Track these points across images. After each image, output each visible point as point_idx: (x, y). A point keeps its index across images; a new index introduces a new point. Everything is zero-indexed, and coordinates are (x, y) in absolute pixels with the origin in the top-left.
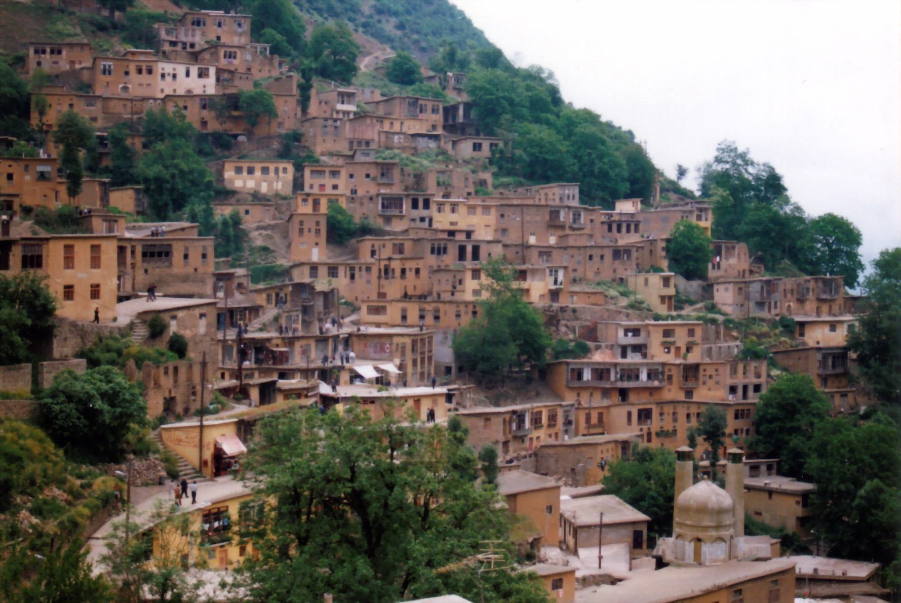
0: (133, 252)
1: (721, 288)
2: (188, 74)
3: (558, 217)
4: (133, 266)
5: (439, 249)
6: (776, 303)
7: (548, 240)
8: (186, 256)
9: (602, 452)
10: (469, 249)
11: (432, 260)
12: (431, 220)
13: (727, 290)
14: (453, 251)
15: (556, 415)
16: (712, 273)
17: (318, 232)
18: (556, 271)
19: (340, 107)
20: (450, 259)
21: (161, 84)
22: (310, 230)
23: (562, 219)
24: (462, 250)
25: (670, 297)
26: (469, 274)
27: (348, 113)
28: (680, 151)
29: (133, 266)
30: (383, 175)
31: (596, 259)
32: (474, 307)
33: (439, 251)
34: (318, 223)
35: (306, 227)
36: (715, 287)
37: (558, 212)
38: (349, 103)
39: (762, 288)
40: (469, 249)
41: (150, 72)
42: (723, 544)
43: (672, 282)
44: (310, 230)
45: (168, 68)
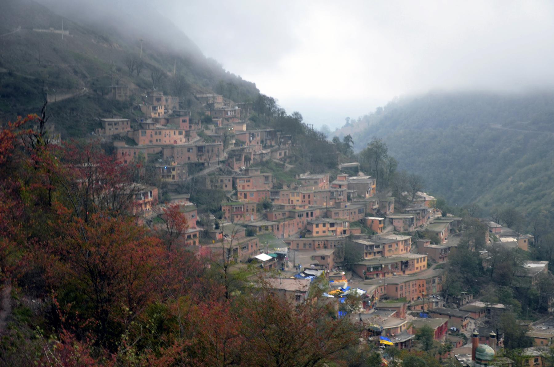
1: (396, 221)
2: (175, 133)
3: (333, 195)
7: (329, 204)
13: (399, 222)
14: (305, 214)
21: (165, 139)
24: (307, 214)
26: (314, 226)
31: (353, 213)
34: (253, 206)
40: (310, 214)
43: (382, 222)
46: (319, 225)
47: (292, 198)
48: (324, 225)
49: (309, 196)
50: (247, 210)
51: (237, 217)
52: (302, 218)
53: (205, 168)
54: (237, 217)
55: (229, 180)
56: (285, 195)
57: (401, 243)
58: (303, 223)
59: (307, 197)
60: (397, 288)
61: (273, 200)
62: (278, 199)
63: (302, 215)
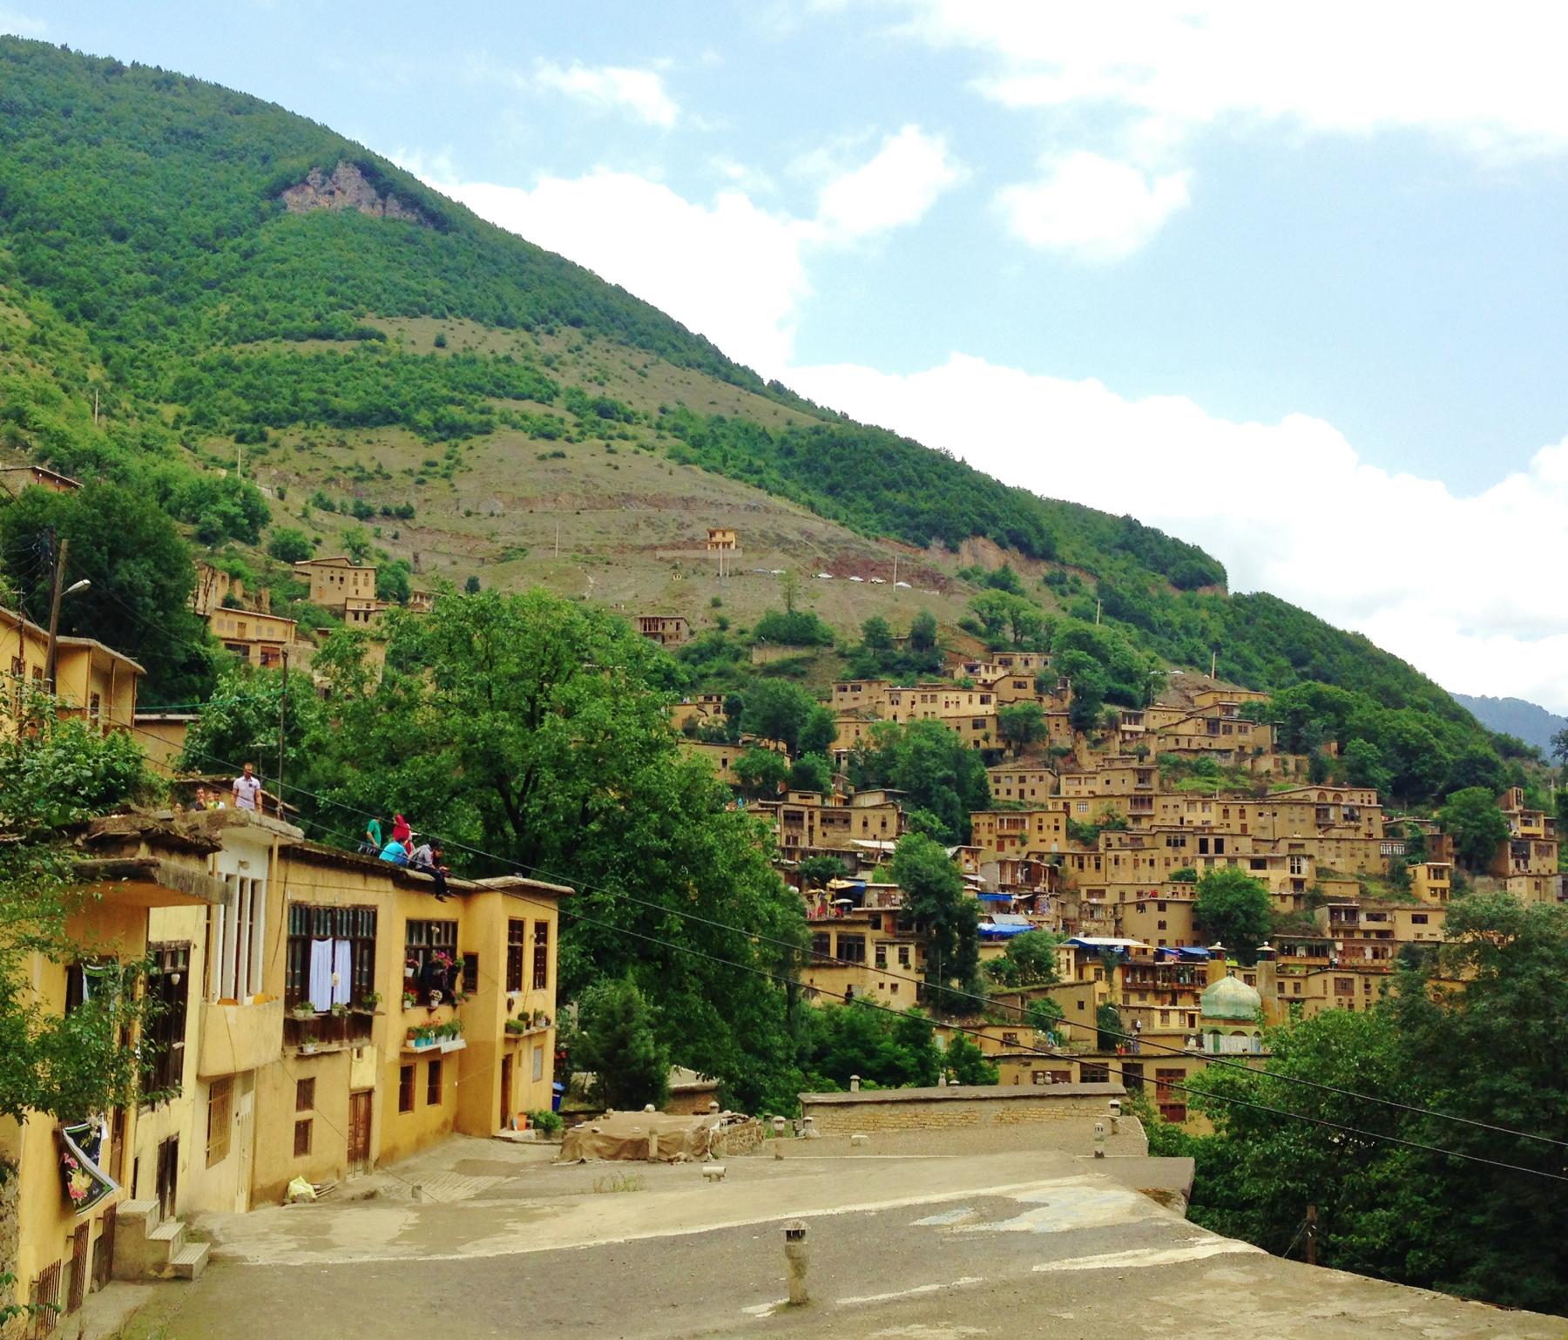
0: (811, 818)
3: (1327, 815)
4: (811, 829)
8: (865, 824)
10: (1211, 842)
11: (1169, 852)
14: (1192, 844)
17: (1057, 828)
19: (1125, 727)
25: (1443, 891)
27: (1137, 733)
29: (811, 829)
30: (1140, 781)
33: (1176, 843)
35: (1044, 825)
40: (1211, 842)
41: (934, 698)
43: (1446, 874)
45: (952, 696)
49: (1242, 812)
50: (1040, 828)
51: (1013, 844)
53: (1005, 761)
54: (1013, 844)
56: (1171, 808)
59: (1234, 811)
61: (1137, 819)
63: (1183, 843)
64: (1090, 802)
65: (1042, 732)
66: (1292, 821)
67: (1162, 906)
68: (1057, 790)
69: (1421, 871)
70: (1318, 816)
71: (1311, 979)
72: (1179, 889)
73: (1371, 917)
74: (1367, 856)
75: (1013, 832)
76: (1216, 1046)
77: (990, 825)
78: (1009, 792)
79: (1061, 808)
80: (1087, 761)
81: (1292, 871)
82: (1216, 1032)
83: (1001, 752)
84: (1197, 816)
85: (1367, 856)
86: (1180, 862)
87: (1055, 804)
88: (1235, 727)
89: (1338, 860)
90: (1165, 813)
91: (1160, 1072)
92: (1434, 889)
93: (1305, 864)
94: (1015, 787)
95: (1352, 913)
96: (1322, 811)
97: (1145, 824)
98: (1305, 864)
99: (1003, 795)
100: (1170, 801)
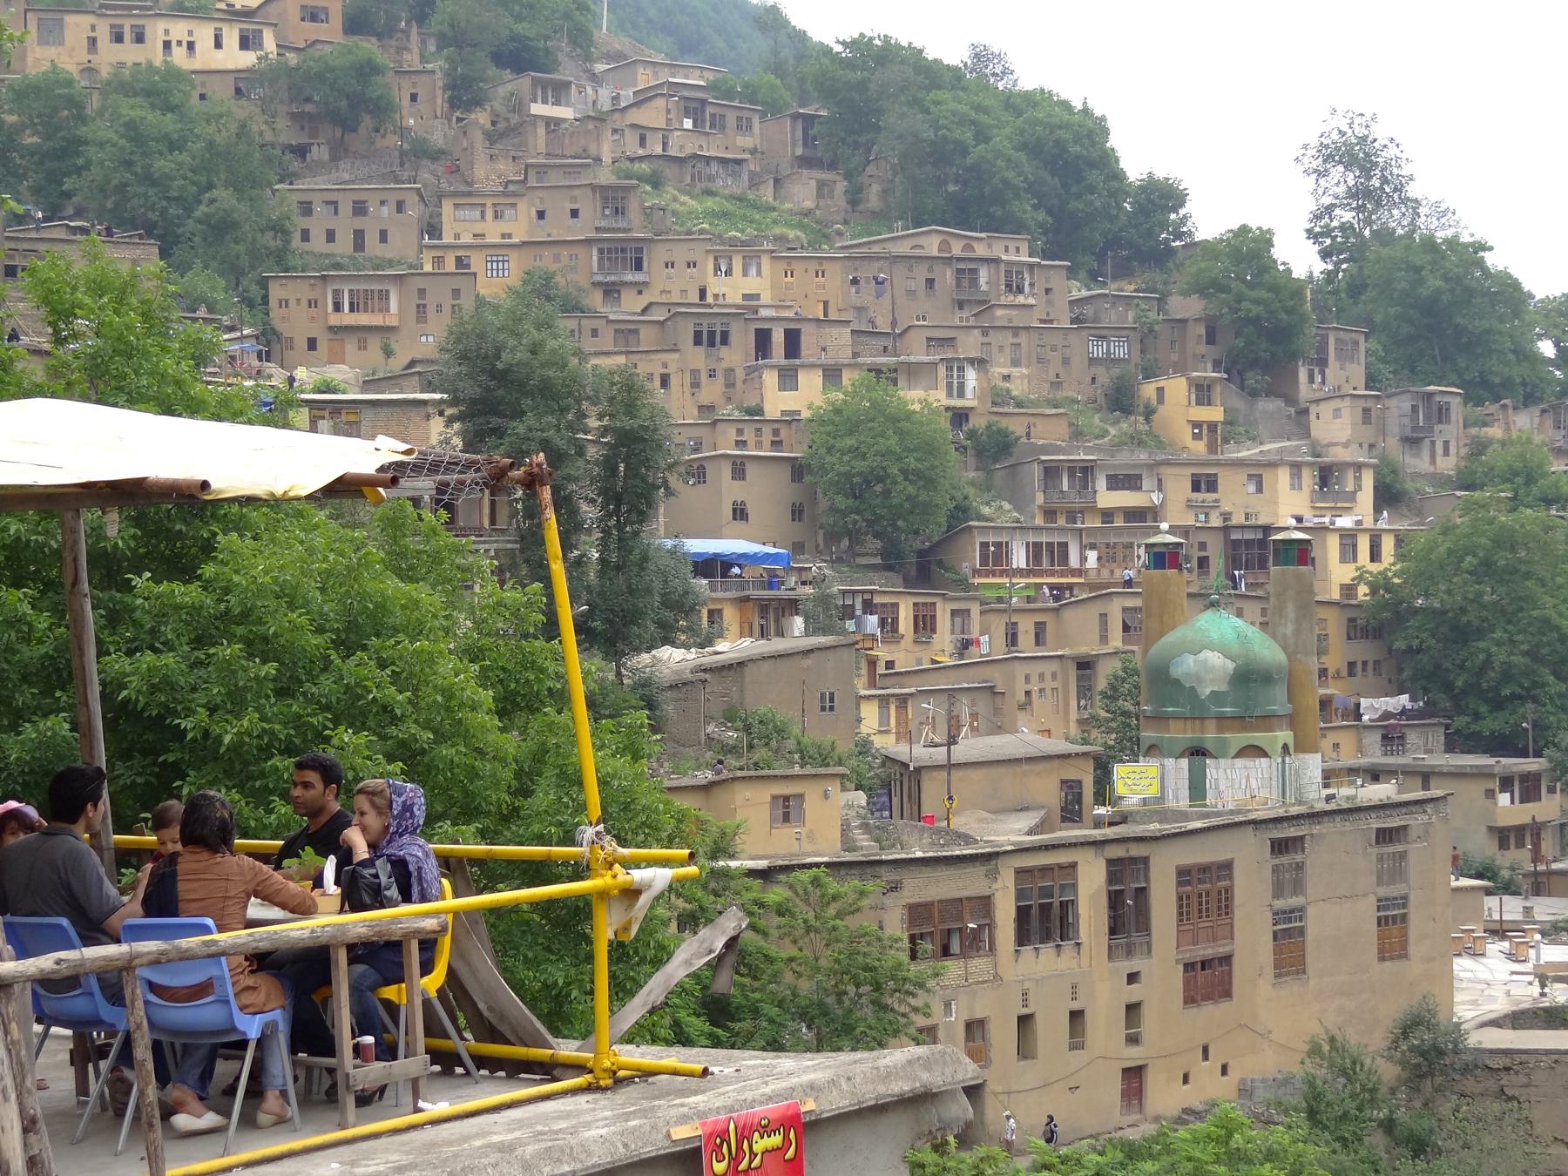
1: (1325, 409)
3: (974, 282)
5: (712, 334)
6: (1446, 443)
9: (1027, 679)
10: (778, 337)
11: (697, 357)
12: (703, 293)
13: (1337, 413)
15: (933, 617)
16: (1304, 391)
18: (961, 369)
19: (537, 109)
20: (737, 354)
22: (439, 308)
23: (984, 287)
24: (763, 341)
25: (1212, 426)
26: (770, 379)
28: (1246, 187)
32: (776, 432)
33: (712, 338)
34: (456, 293)
35: (430, 301)
36: (1313, 409)
37: (974, 271)
38: (557, 103)
39: (1414, 408)
40: (778, 337)
42: (1263, 760)
44: (439, 308)
46: (802, 377)
47: (716, 285)
48: (832, 374)
50: (421, 308)
51: (363, 347)
52: (724, 351)
54: (363, 347)
55: (400, 207)
57: (1284, 476)
58: (730, 385)
60: (1104, 617)
61: (611, 291)
62: (640, 288)
63: (725, 339)
64: (514, 256)
65: (382, 110)
66: (911, 293)
67: (739, 471)
68: (434, 230)
69: (1177, 388)
70: (958, 285)
71: (1068, 614)
72: (749, 435)
73: (1115, 483)
74: (1066, 362)
75: (363, 319)
76: (1197, 788)
77: (313, 303)
78: (331, 236)
79: (450, 266)
80: (488, 172)
81: (950, 395)
82: (1198, 752)
83: (301, 151)
84: (731, 288)
85: (1066, 362)
86: (720, 380)
87: (439, 261)
88: (731, 120)
89: (1015, 371)
90: (669, 281)
91: (1184, 875)
92: (1196, 425)
93: (971, 376)
94: (345, 227)
95: (1085, 472)
96: (966, 274)
97: (631, 304)
98: (971, 376)
99: (318, 243)
100: (681, 254)
